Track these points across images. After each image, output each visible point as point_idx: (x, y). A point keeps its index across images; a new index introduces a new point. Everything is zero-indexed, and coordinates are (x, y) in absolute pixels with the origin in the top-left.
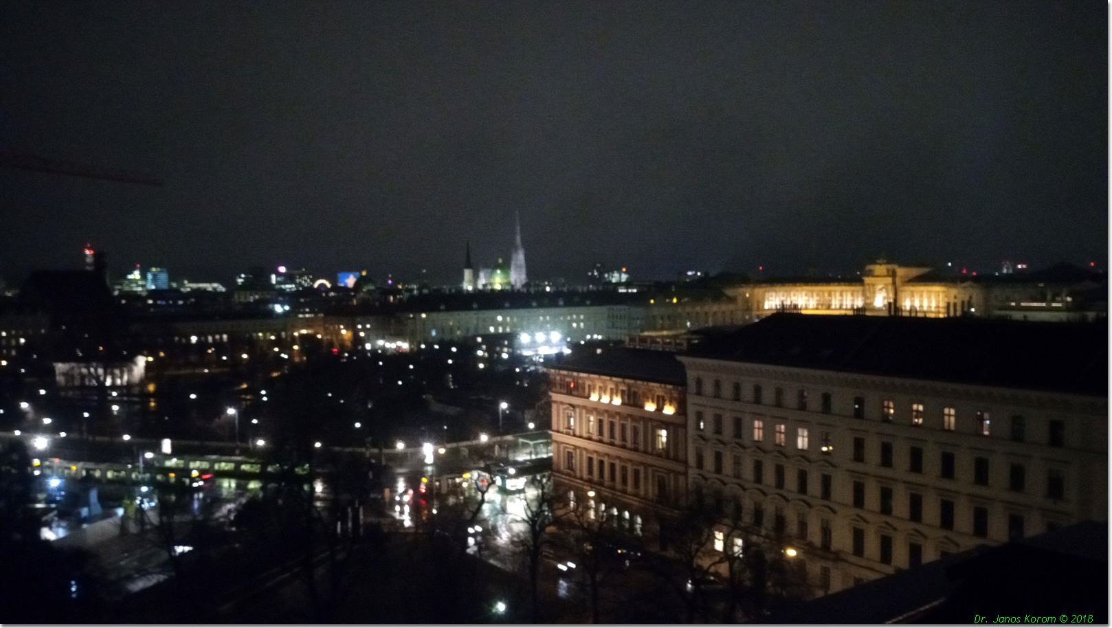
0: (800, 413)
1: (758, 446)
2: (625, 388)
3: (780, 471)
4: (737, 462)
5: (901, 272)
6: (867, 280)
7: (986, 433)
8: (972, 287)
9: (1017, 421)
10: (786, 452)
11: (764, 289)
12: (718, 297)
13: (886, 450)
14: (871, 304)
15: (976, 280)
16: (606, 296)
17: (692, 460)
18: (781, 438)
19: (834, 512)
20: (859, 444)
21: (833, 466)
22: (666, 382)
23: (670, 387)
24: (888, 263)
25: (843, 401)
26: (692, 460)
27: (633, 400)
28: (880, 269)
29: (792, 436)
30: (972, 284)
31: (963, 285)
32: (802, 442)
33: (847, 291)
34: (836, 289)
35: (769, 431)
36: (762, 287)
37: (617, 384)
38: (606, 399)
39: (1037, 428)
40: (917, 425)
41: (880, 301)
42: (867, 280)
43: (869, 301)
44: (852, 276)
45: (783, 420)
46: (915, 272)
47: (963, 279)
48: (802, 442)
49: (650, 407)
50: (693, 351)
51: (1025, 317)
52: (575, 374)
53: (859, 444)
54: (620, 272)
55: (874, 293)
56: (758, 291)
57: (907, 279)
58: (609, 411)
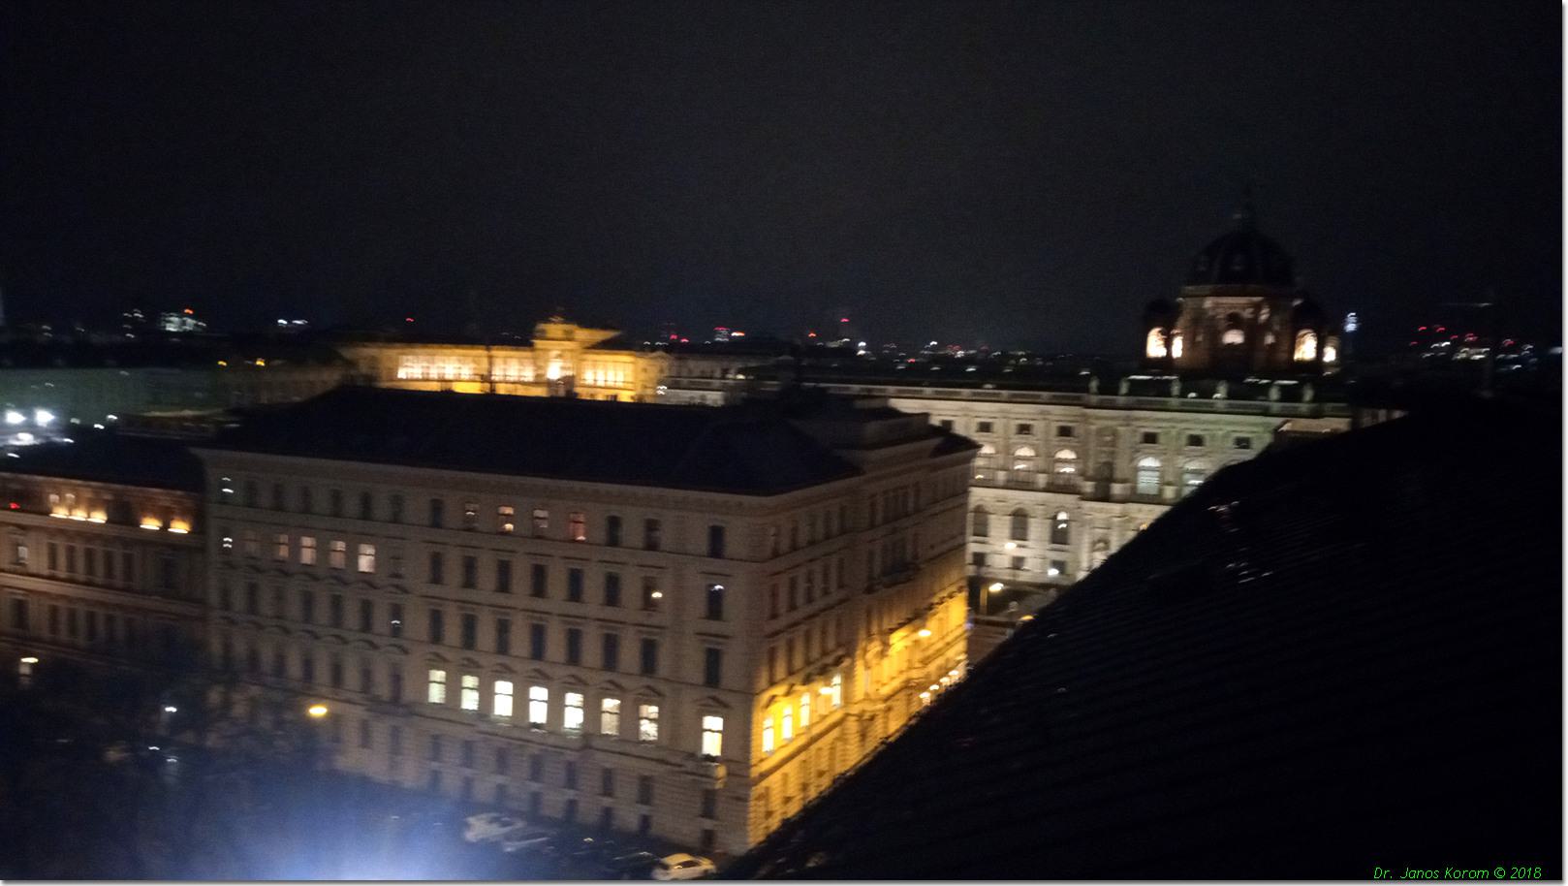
0: (363, 522)
1: (309, 572)
2: (108, 497)
3: (337, 603)
4: (279, 597)
5: (583, 335)
6: (539, 343)
7: (581, 538)
8: (662, 358)
9: (614, 523)
10: (345, 577)
11: (400, 351)
12: (328, 359)
13: (470, 567)
14: (543, 375)
15: (668, 349)
16: (156, 351)
17: (214, 598)
18: (338, 560)
19: (405, 652)
20: (437, 562)
21: (405, 591)
22: (174, 487)
23: (179, 493)
24: (563, 323)
25: (417, 507)
26: (214, 598)
27: (124, 515)
28: (555, 329)
29: (352, 556)
30: (664, 354)
31: (654, 354)
32: (365, 563)
33: (511, 357)
34: (499, 353)
35: (323, 550)
36: (395, 348)
37: (96, 491)
38: (79, 515)
39: (632, 533)
40: (507, 533)
41: (555, 371)
42: (539, 343)
43: (540, 372)
44: (520, 337)
45: (340, 534)
46: (600, 335)
47: (653, 349)
48: (365, 563)
49: (151, 524)
50: (225, 440)
51: (703, 398)
52: (25, 477)
53: (437, 562)
54: (182, 315)
55: (547, 361)
56: (386, 354)
57: (587, 345)
58: (85, 531)
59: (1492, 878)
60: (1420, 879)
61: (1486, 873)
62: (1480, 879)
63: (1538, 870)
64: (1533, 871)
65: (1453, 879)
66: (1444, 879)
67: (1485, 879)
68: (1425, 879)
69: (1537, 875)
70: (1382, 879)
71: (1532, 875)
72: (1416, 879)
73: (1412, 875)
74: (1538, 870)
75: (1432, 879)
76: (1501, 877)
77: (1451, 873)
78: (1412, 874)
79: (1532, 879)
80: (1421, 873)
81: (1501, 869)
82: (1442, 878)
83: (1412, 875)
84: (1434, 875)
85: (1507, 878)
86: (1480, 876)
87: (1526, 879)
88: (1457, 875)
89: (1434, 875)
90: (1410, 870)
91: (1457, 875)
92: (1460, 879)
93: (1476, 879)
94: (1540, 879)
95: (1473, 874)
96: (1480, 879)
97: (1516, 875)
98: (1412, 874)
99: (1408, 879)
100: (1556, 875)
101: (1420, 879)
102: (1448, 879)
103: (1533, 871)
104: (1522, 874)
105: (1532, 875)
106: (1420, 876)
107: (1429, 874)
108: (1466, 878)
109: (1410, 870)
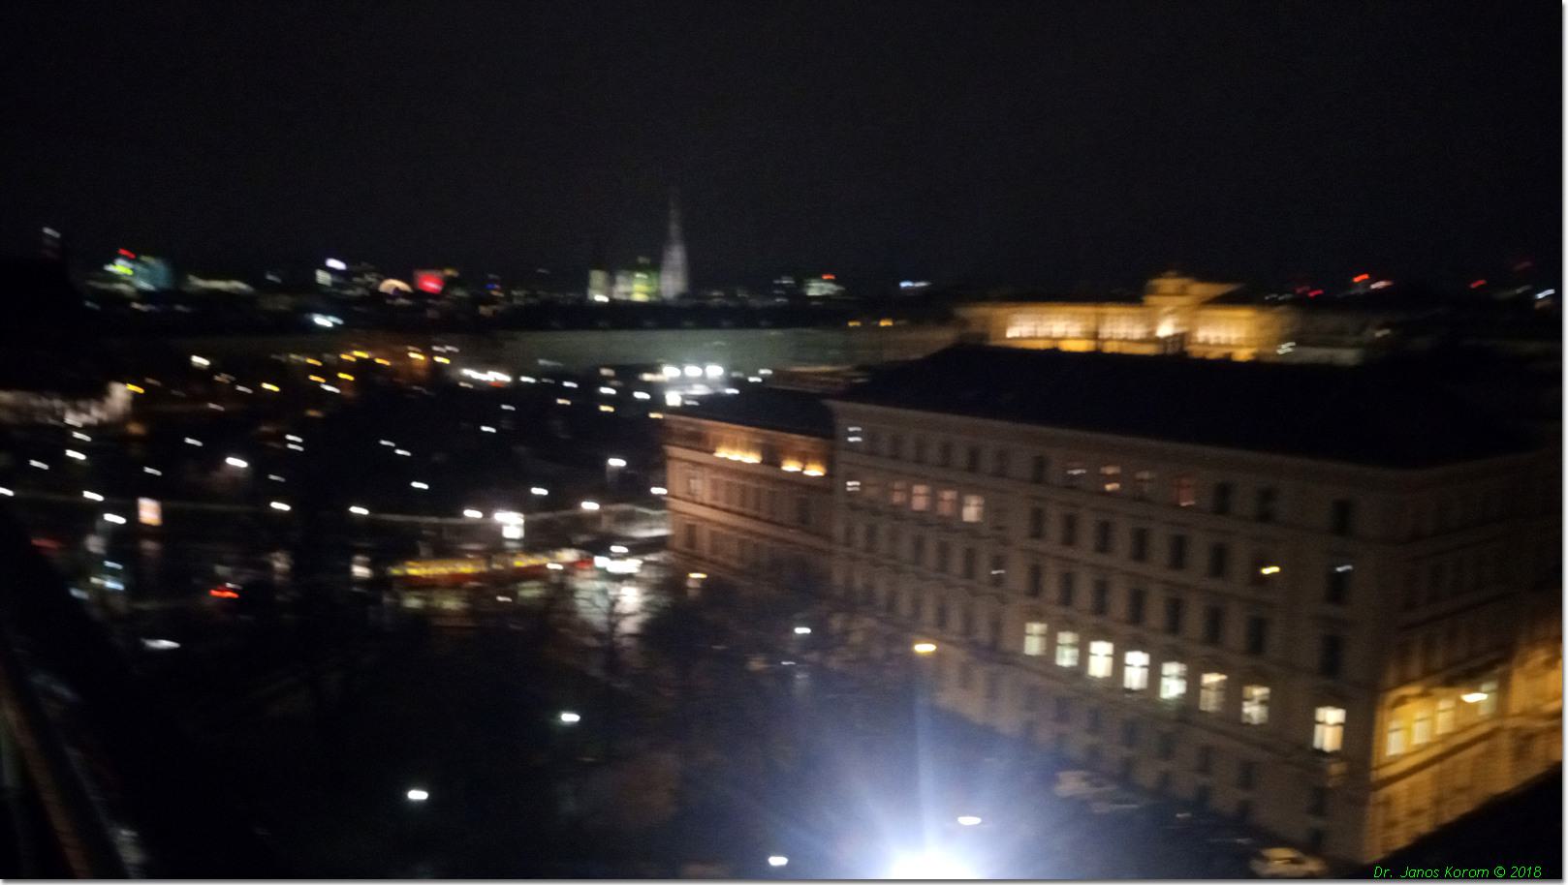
59: (1492, 877)
60: (1420, 878)
61: (1486, 872)
62: (1480, 878)
63: (1538, 869)
64: (1533, 870)
65: (1453, 878)
66: (1444, 878)
67: (1484, 878)
68: (1425, 878)
69: (1537, 874)
70: (1382, 878)
71: (1532, 874)
72: (1416, 878)
73: (1412, 874)
74: (1538, 869)
75: (1432, 878)
76: (1501, 876)
77: (1451, 872)
78: (1412, 873)
79: (1532, 878)
80: (1421, 872)
81: (1501, 868)
82: (1442, 877)
83: (1412, 874)
84: (1434, 874)
85: (1507, 877)
86: (1480, 875)
87: (1526, 878)
88: (1457, 873)
89: (1434, 874)
90: (1410, 869)
91: (1457, 873)
92: (1460, 878)
93: (1476, 878)
94: (1540, 878)
95: (1473, 873)
96: (1480, 878)
97: (1516, 874)
98: (1412, 873)
99: (1408, 878)
100: (1556, 874)
101: (1420, 878)
102: (1448, 877)
103: (1533, 870)
104: (1522, 873)
105: (1532, 874)
106: (1420, 875)
107: (1429, 873)
108: (1466, 877)
109: (1410, 869)
